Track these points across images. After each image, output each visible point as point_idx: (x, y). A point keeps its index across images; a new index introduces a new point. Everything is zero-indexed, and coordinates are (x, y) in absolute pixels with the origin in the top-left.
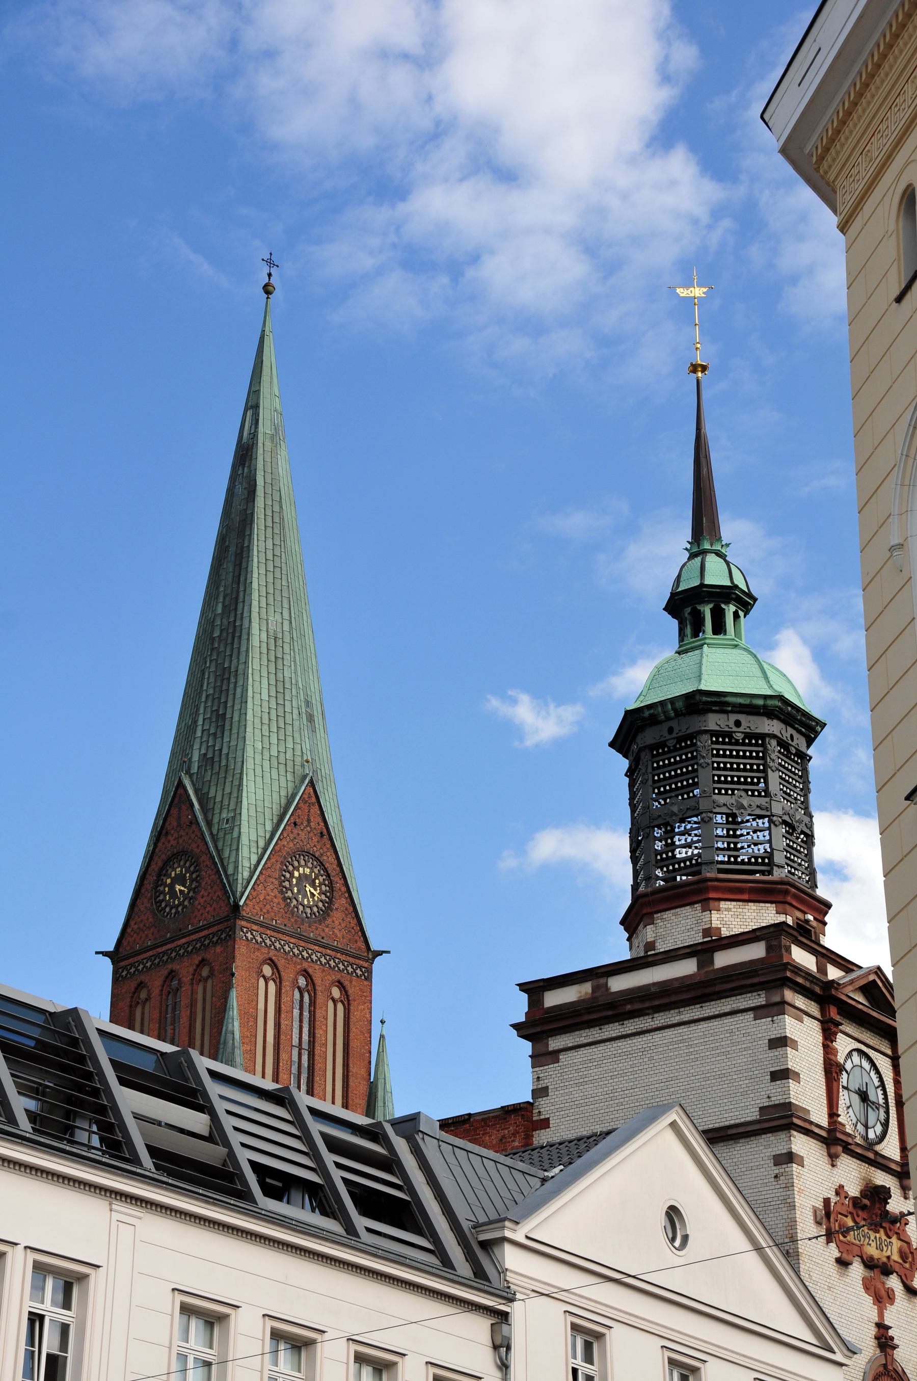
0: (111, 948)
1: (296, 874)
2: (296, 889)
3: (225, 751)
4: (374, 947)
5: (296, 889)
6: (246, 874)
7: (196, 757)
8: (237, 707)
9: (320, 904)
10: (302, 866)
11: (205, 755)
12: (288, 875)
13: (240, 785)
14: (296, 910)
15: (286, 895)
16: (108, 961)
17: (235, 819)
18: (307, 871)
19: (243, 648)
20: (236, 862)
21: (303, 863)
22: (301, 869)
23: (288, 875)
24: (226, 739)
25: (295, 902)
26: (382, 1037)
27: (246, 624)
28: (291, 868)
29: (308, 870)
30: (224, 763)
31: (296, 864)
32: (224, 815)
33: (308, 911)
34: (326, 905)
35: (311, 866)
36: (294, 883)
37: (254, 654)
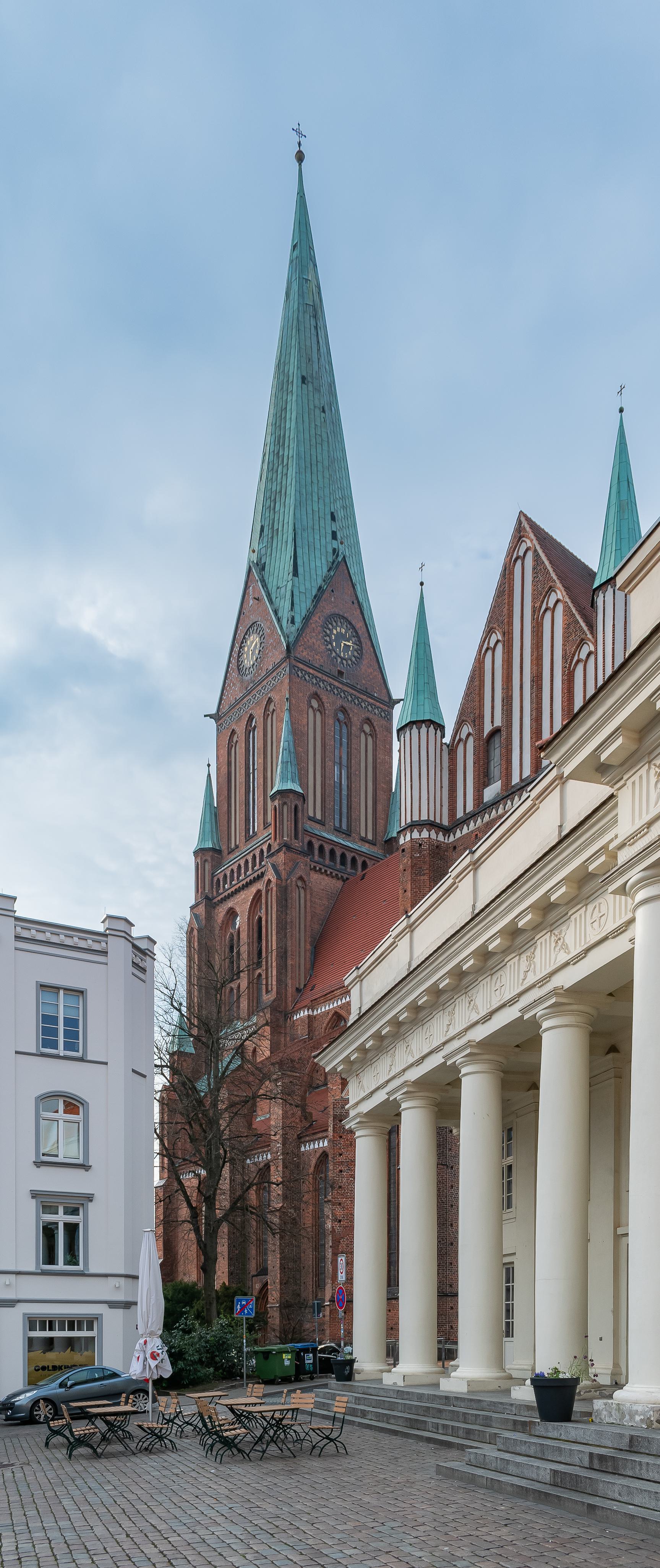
1: (335, 632)
2: (334, 643)
5: (334, 643)
9: (354, 659)
10: (339, 627)
12: (328, 632)
14: (335, 660)
15: (328, 647)
18: (343, 631)
21: (339, 624)
22: (338, 629)
23: (328, 632)
25: (334, 654)
28: (330, 626)
29: (344, 631)
31: (334, 624)
33: (344, 662)
34: (358, 660)
35: (345, 628)
36: (333, 638)
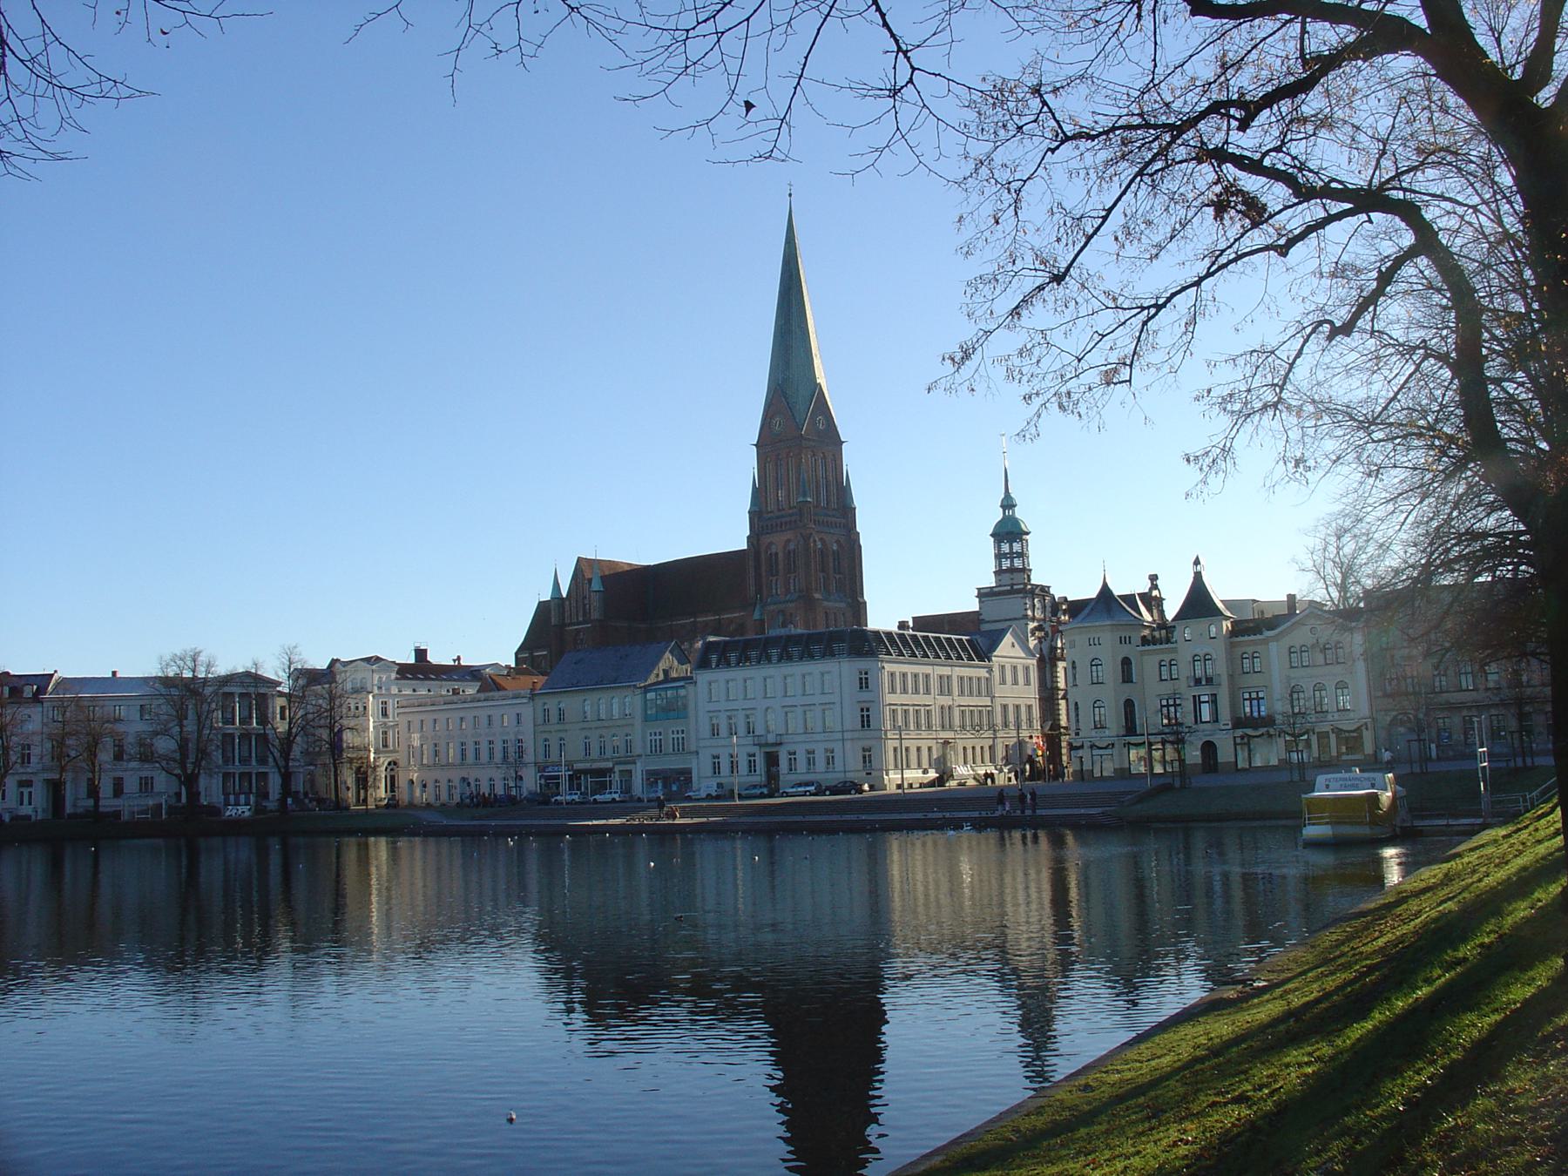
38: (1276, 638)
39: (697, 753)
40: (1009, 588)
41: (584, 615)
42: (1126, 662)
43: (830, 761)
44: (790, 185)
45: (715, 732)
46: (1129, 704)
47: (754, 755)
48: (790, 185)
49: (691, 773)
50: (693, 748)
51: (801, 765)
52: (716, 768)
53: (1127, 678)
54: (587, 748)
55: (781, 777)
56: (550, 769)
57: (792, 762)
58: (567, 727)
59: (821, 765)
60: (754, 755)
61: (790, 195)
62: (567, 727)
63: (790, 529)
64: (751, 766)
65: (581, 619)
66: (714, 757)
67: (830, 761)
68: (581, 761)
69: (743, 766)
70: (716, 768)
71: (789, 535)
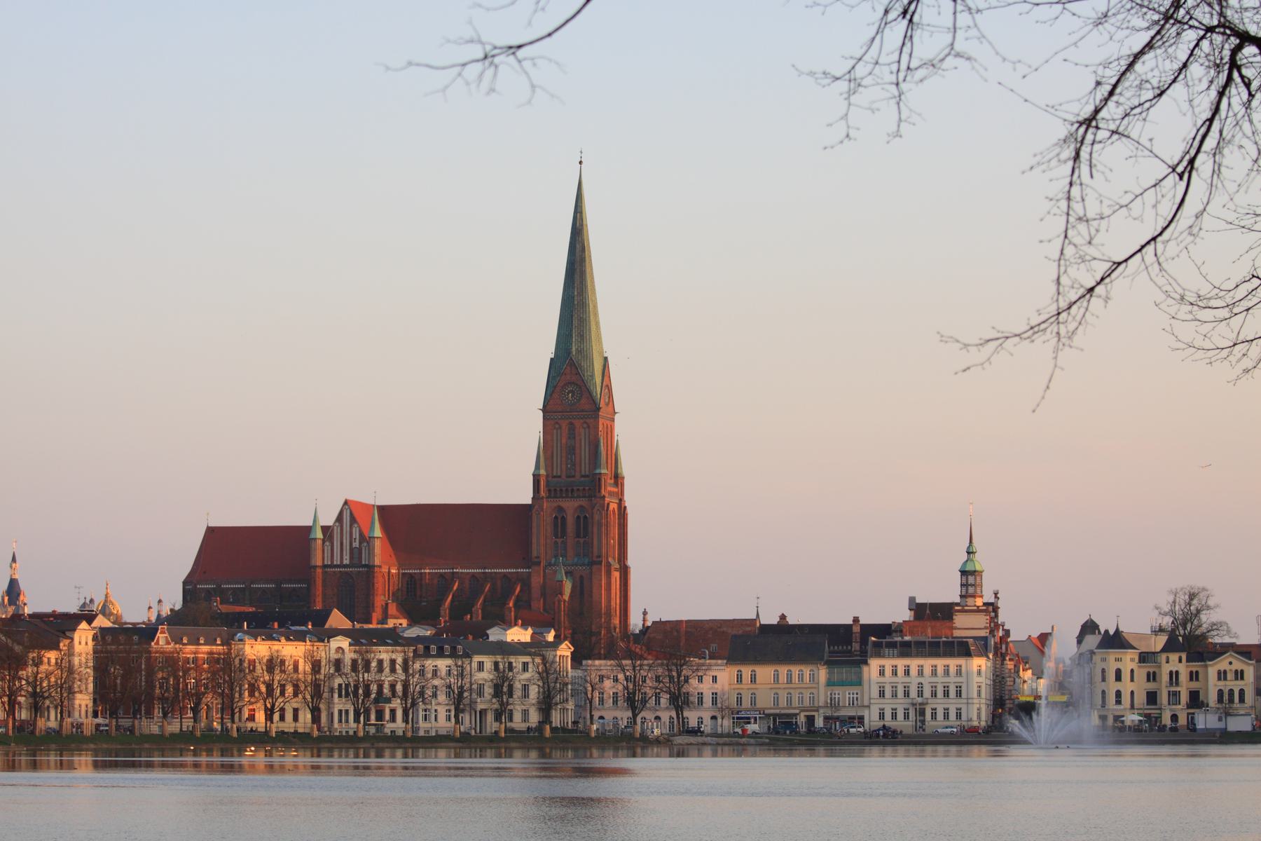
0: (541, 408)
3: (585, 349)
4: (616, 411)
6: (599, 396)
7: (574, 349)
8: (588, 333)
11: (578, 349)
13: (593, 364)
16: (541, 412)
17: (592, 376)
19: (588, 312)
20: (596, 392)
24: (585, 344)
26: (617, 441)
27: (587, 302)
30: (585, 354)
32: (589, 373)
37: (591, 314)
38: (1211, 665)
39: (868, 707)
40: (975, 608)
41: (351, 558)
42: (1132, 671)
43: (959, 715)
44: (581, 152)
45: (882, 694)
46: (1132, 693)
47: (908, 709)
48: (581, 152)
49: (863, 719)
50: (866, 703)
51: (940, 716)
52: (882, 716)
53: (1132, 680)
54: (776, 700)
55: (926, 723)
56: (743, 713)
57: (934, 716)
58: (757, 686)
59: (953, 716)
60: (908, 709)
61: (581, 163)
62: (757, 686)
63: (584, 497)
64: (906, 716)
65: (346, 562)
66: (880, 709)
67: (959, 715)
68: (771, 708)
69: (900, 716)
70: (882, 716)
71: (583, 502)
